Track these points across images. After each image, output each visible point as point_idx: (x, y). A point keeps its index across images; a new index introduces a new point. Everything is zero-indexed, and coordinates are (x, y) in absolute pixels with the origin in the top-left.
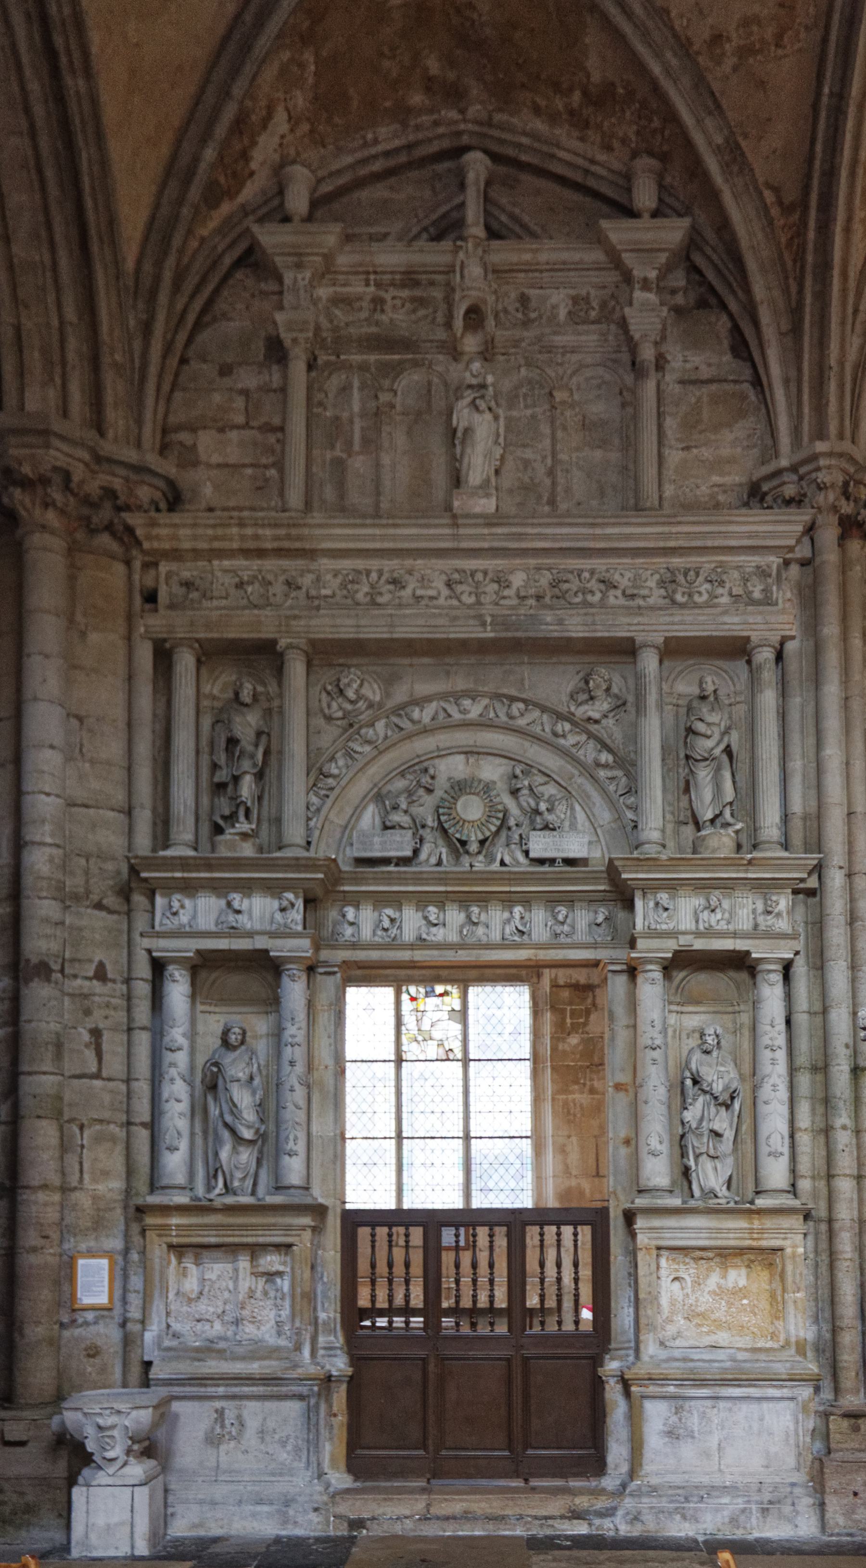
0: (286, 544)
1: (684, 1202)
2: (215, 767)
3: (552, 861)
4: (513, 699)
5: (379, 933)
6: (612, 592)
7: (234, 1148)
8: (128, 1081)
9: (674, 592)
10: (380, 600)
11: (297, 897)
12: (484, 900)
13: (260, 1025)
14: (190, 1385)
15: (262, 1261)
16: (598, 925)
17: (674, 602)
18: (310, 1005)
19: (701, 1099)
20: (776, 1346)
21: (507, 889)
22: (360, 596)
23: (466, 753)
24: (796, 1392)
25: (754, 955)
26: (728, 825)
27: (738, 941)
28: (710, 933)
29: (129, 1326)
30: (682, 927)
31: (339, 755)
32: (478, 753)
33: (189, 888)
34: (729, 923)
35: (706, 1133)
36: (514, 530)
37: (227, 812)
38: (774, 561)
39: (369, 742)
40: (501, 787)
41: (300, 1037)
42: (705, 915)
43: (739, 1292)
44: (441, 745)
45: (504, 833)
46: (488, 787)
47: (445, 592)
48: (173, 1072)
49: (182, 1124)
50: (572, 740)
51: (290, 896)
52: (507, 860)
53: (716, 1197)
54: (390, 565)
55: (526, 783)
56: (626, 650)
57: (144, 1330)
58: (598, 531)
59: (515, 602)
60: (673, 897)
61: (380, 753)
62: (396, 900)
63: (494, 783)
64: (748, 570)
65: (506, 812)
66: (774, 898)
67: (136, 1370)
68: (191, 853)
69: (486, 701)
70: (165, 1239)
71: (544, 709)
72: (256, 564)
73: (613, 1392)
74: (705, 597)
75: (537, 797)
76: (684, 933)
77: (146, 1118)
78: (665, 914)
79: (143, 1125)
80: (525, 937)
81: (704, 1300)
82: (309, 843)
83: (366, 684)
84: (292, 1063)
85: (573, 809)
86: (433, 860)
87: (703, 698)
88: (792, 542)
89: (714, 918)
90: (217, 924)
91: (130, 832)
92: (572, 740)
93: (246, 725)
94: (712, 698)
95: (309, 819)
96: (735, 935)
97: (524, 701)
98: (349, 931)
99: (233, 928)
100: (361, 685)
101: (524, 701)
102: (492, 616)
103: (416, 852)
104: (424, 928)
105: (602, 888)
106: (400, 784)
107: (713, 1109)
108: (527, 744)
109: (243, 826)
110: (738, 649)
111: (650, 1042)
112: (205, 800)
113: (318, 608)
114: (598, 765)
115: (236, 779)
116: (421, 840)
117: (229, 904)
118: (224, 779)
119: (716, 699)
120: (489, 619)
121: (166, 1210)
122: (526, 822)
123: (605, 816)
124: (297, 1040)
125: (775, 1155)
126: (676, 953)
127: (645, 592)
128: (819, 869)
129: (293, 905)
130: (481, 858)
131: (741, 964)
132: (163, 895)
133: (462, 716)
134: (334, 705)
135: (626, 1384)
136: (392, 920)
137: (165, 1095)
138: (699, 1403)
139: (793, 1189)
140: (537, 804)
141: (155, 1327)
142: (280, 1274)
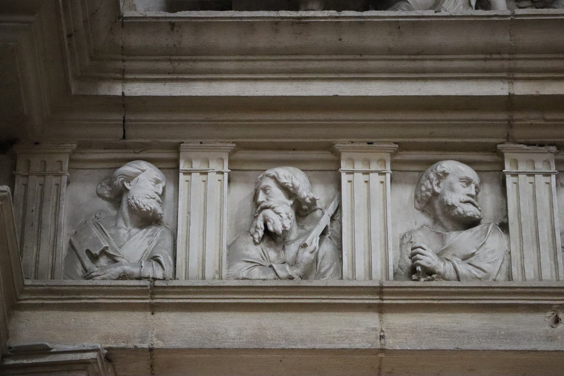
5: (254, 252)
62: (317, 138)
136: (303, 210)
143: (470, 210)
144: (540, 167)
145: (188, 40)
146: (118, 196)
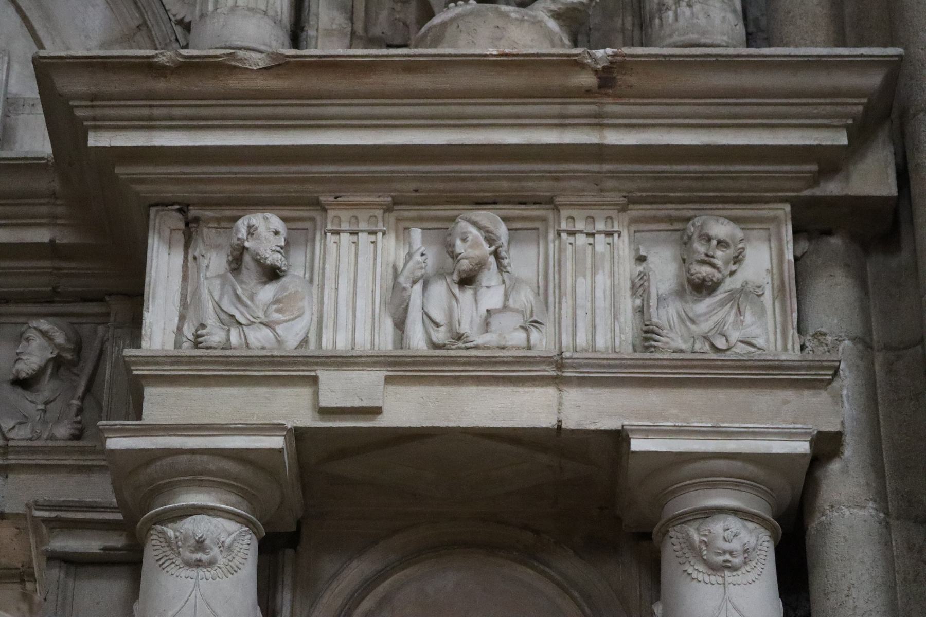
16: (24, 383)
25: (638, 444)
27: (573, 395)
28: (450, 364)
30: (337, 340)
60: (299, 235)
78: (268, 292)
89: (468, 310)
96: (560, 371)
105: (42, 236)
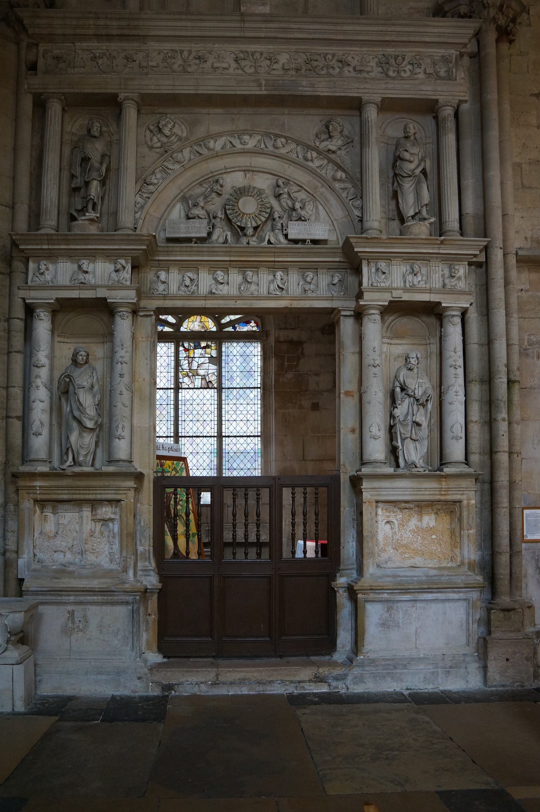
0: (126, 32)
1: (395, 471)
2: (73, 176)
3: (304, 241)
4: (277, 136)
6: (346, 69)
7: (80, 433)
8: (7, 388)
9: (388, 70)
10: (189, 69)
11: (127, 263)
12: (256, 266)
13: (98, 351)
14: (50, 595)
15: (99, 511)
17: (387, 76)
18: (134, 337)
19: (407, 401)
20: (454, 565)
21: (273, 259)
22: (175, 67)
23: (244, 171)
24: (469, 595)
25: (443, 305)
26: (425, 219)
27: (432, 295)
28: (413, 289)
29: (8, 554)
30: (395, 285)
31: (157, 170)
32: (253, 171)
33: (52, 256)
34: (426, 283)
35: (410, 424)
36: (282, 25)
37: (79, 208)
38: (453, 52)
39: (178, 162)
40: (269, 192)
41: (127, 358)
42: (410, 278)
43: (430, 530)
44: (227, 166)
45: (269, 224)
46: (260, 192)
47: (234, 65)
48: (39, 382)
49: (45, 418)
50: (317, 163)
51: (123, 262)
52: (273, 240)
53: (416, 467)
54: (195, 47)
55: (286, 190)
56: (356, 105)
57: (18, 558)
58: (339, 28)
59: (281, 72)
60: (388, 266)
61: (186, 170)
62: (195, 266)
63: (264, 190)
64: (436, 58)
65: (272, 208)
66: (457, 267)
67: (13, 584)
68: (53, 232)
69: (258, 137)
70: (31, 495)
71: (298, 143)
72: (104, 46)
73: (342, 598)
74: (408, 73)
75: (293, 201)
76: (396, 289)
77: (19, 413)
78: (383, 276)
79: (18, 418)
80: (284, 292)
81: (407, 536)
82: (136, 228)
83: (177, 125)
84: (121, 376)
85: (317, 208)
86: (221, 240)
87: (407, 137)
88: (467, 41)
89: (416, 280)
90: (71, 281)
91: (13, 220)
92: (317, 163)
93: (95, 150)
94: (412, 138)
95: (136, 213)
96: (430, 291)
97: (285, 137)
98: (161, 287)
99: (82, 283)
100: (174, 126)
101: (285, 137)
102: (265, 80)
103: (210, 234)
104: (213, 286)
105: (338, 259)
106: (199, 190)
107: (415, 408)
108: (286, 166)
109: (91, 215)
110: (430, 108)
111: (372, 362)
112: (65, 200)
113: (147, 74)
114: (335, 179)
115: (87, 184)
116: (214, 226)
117: (80, 267)
118: (78, 185)
119: (415, 139)
120: (264, 83)
121: (33, 476)
122: (286, 216)
123: (339, 213)
124: (124, 359)
125: (457, 438)
126: (391, 302)
127: (369, 69)
128: (486, 249)
129: (124, 268)
130: (254, 239)
131: (433, 312)
132: (34, 262)
133: (242, 147)
134: (155, 139)
135: (352, 592)
136: (192, 280)
137: (32, 398)
138: (403, 604)
139: (467, 461)
140: (294, 205)
141: (25, 556)
142: (111, 520)
143: (222, 281)
144: (235, 272)
145: (170, 249)
146: (158, 277)
